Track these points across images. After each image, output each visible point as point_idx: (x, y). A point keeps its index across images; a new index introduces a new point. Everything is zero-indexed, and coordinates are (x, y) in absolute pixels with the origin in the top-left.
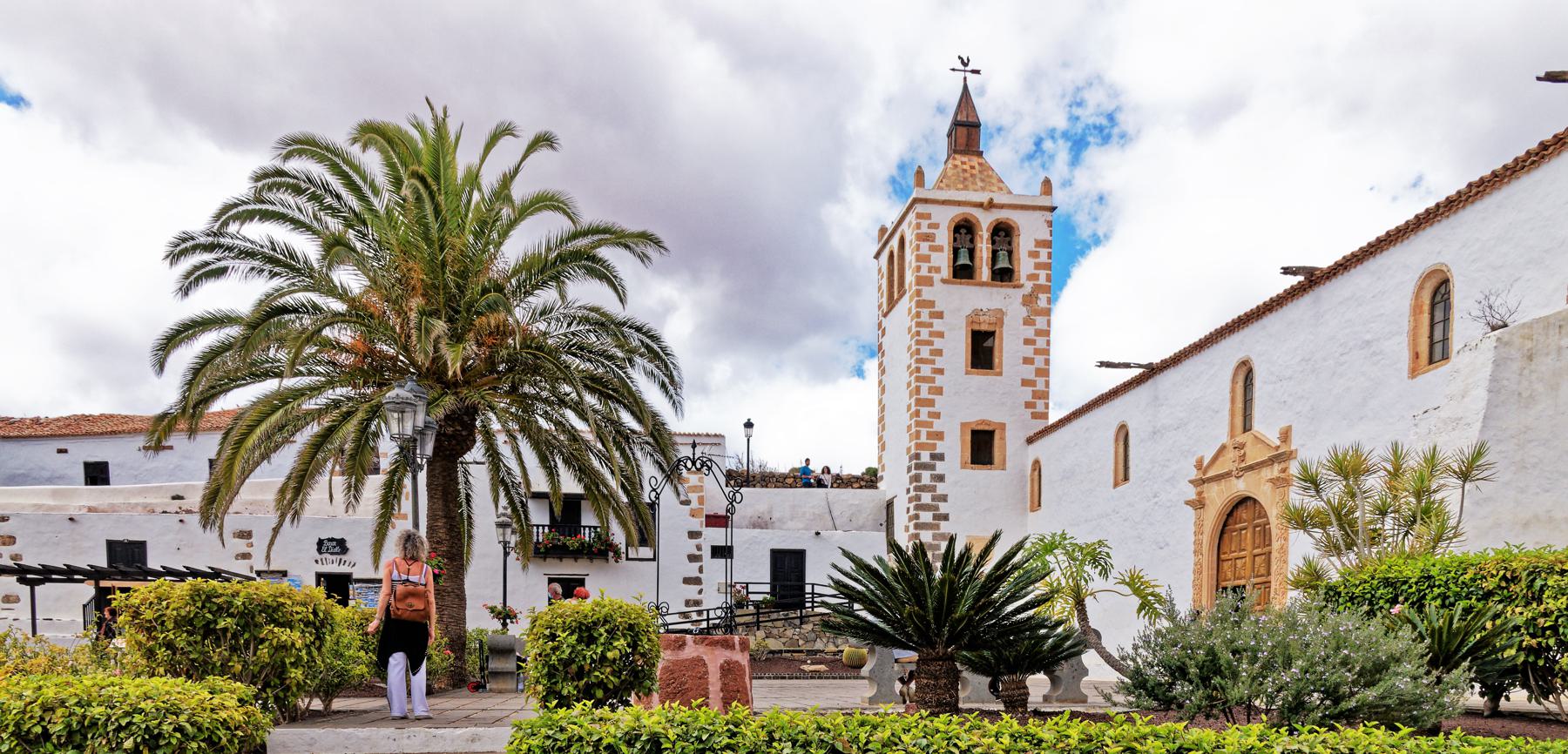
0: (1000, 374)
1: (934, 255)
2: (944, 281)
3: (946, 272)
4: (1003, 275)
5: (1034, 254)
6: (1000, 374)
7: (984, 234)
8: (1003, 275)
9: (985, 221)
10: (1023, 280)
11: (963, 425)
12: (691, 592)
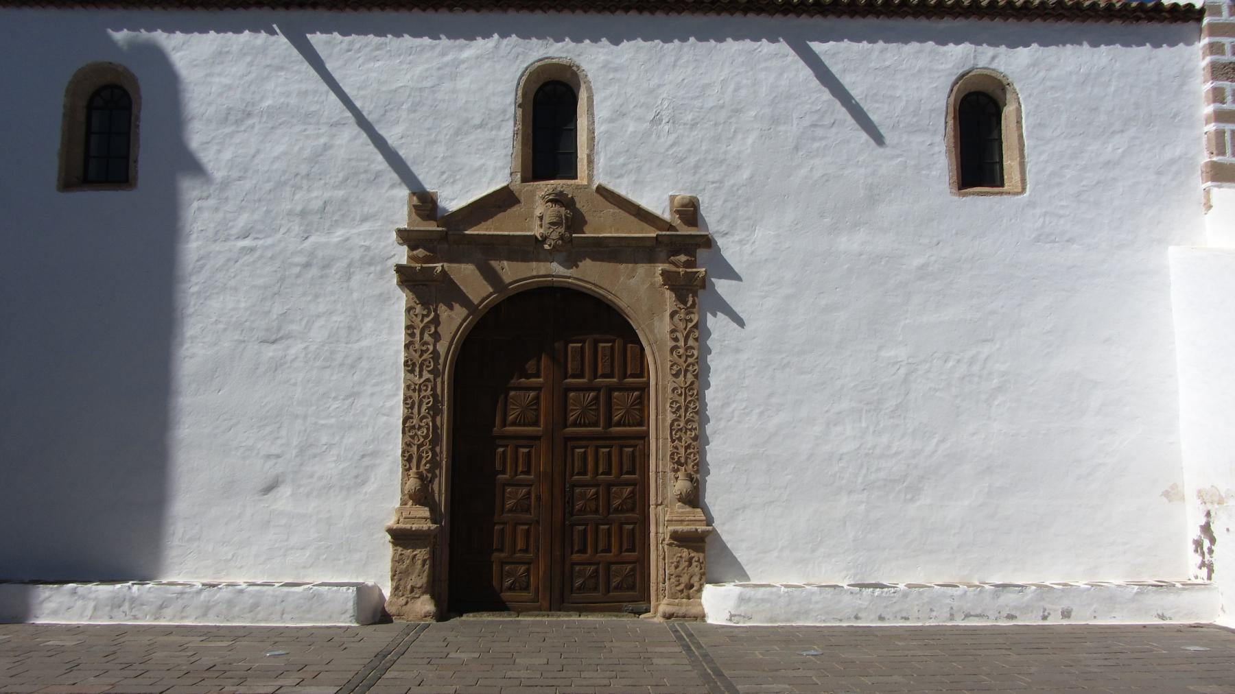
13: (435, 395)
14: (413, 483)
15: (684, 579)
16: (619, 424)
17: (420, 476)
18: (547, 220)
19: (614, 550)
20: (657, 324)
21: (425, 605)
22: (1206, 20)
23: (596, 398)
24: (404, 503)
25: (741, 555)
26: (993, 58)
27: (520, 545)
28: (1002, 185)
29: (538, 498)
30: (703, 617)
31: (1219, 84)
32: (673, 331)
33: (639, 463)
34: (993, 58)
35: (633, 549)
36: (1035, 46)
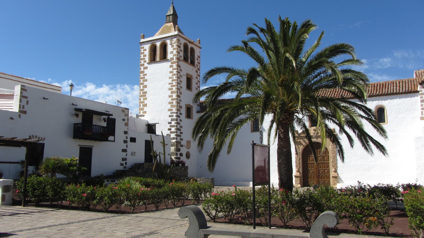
0: (192, 91)
1: (181, 52)
2: (182, 60)
3: (182, 58)
4: (192, 63)
5: (197, 59)
6: (192, 91)
7: (189, 50)
8: (192, 63)
9: (190, 46)
10: (196, 65)
11: (186, 105)
12: (123, 155)
13: (299, 158)
14: (297, 169)
15: (334, 183)
16: (326, 161)
17: (298, 169)
18: (313, 133)
19: (326, 179)
20: (330, 147)
21: (299, 185)
22: (420, 93)
23: (322, 157)
24: (296, 172)
25: (343, 179)
26: (382, 103)
27: (312, 178)
28: (385, 122)
29: (315, 171)
30: (337, 188)
31: (422, 103)
32: (332, 148)
33: (328, 167)
34: (382, 103)
35: (328, 179)
36: (389, 100)
